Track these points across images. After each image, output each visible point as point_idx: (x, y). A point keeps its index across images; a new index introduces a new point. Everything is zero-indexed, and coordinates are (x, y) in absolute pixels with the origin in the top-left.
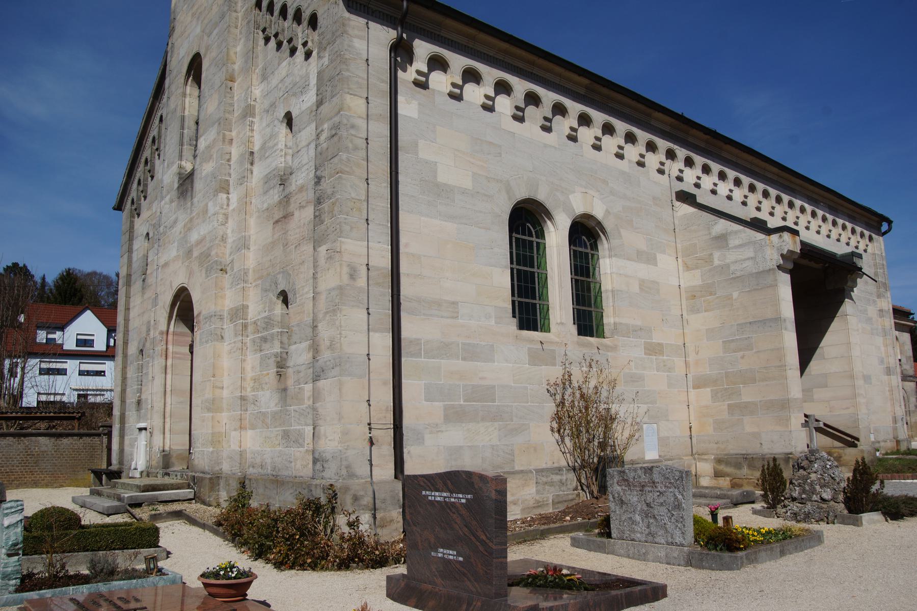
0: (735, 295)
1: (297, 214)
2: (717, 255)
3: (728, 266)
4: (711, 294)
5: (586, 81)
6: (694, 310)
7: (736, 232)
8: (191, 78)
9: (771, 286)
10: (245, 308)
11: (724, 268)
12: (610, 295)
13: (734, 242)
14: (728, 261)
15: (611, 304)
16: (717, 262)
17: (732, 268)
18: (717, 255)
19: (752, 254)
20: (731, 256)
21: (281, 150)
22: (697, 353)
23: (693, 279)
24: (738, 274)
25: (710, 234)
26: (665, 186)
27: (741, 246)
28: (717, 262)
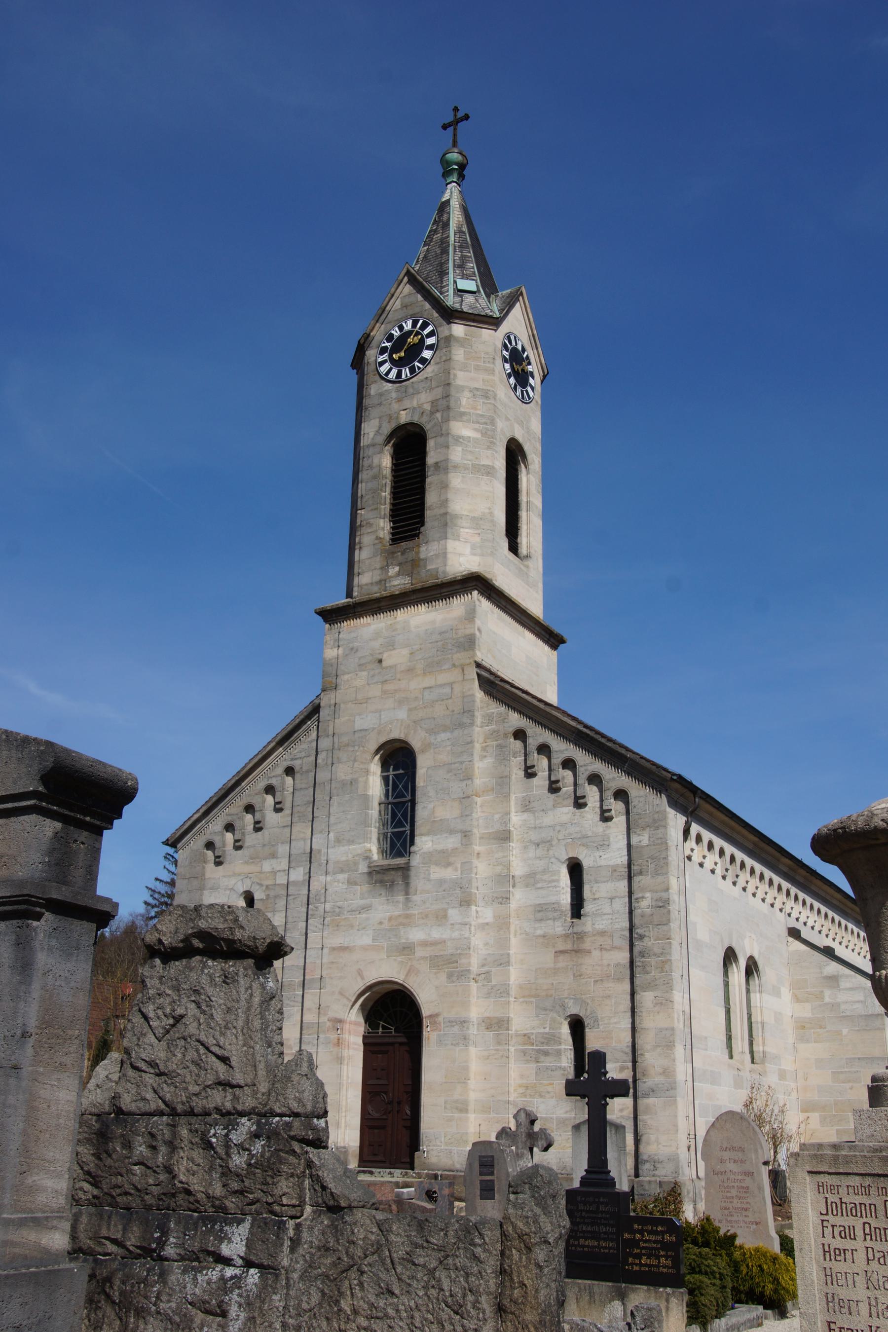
0: (845, 1031)
1: (596, 954)
2: (827, 993)
3: (838, 1005)
4: (821, 1027)
5: (755, 839)
6: (802, 1039)
7: (847, 976)
8: (378, 757)
9: (879, 1029)
10: (508, 1020)
11: (834, 1006)
12: (760, 1025)
13: (844, 984)
14: (838, 1000)
15: (760, 1034)
16: (827, 1000)
17: (843, 1007)
18: (827, 993)
19: (862, 998)
20: (841, 997)
21: (563, 888)
22: (806, 1080)
23: (805, 1011)
24: (848, 1014)
25: (821, 973)
26: (781, 923)
27: (851, 989)
28: (827, 1000)
